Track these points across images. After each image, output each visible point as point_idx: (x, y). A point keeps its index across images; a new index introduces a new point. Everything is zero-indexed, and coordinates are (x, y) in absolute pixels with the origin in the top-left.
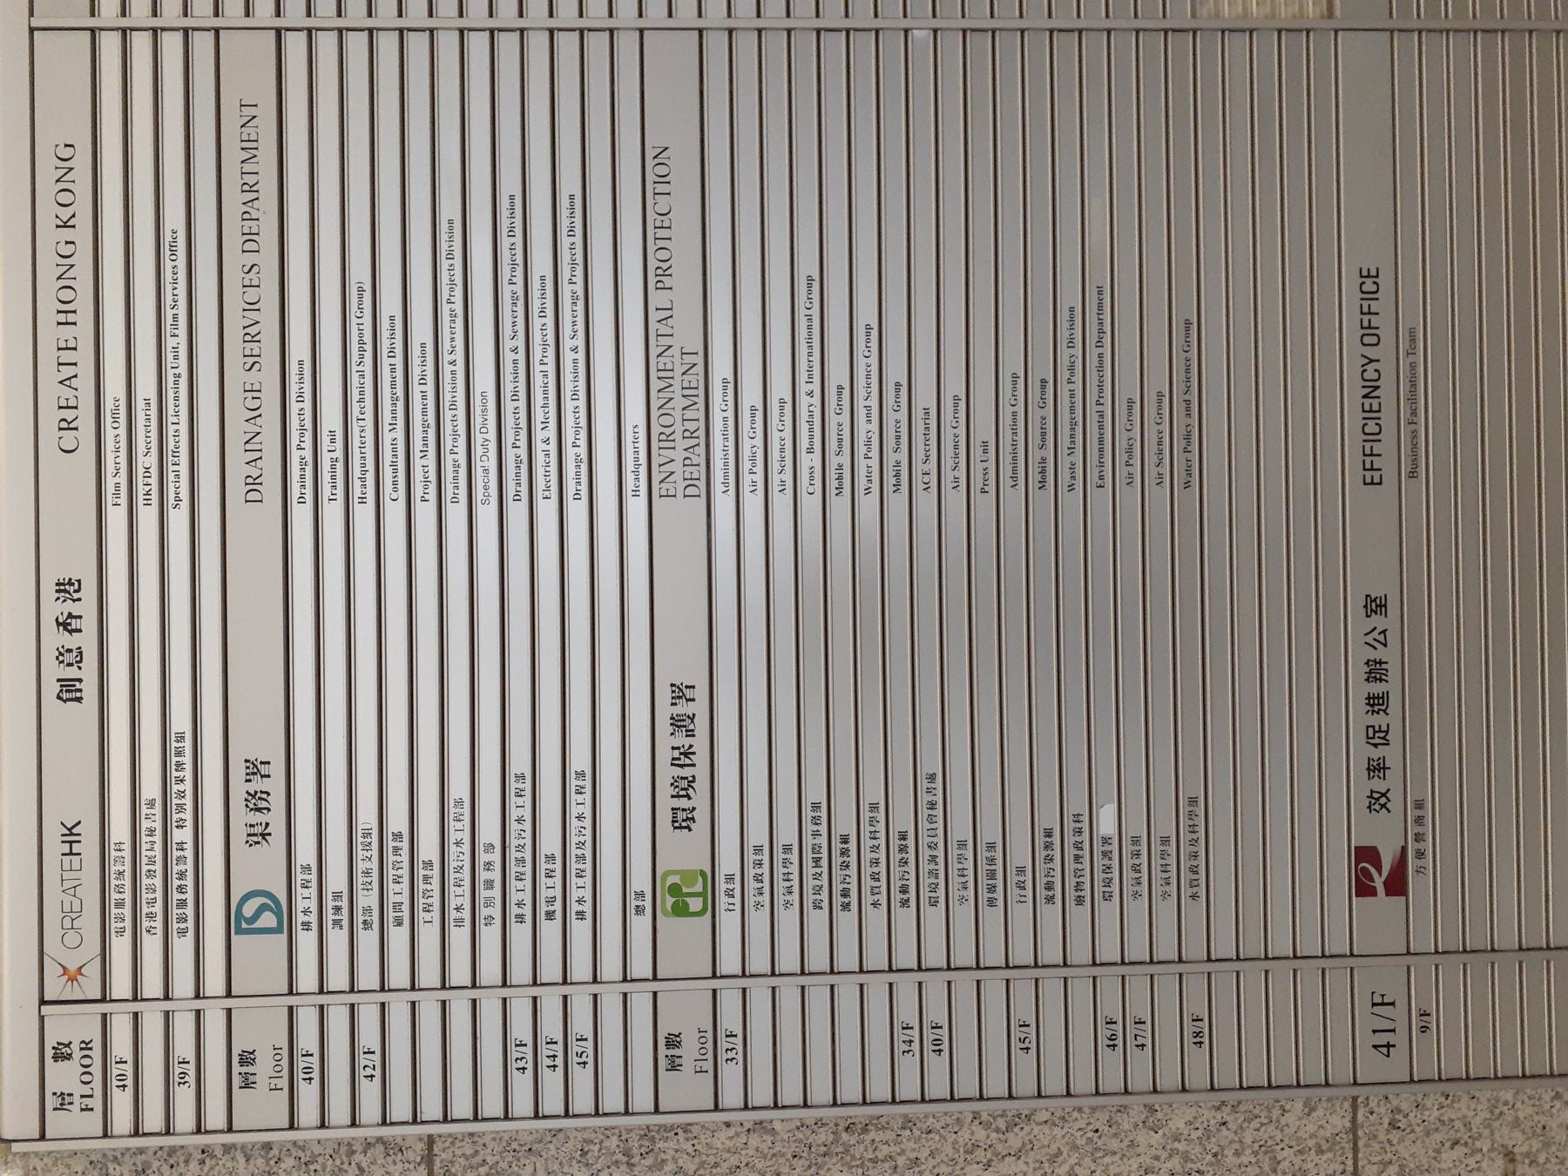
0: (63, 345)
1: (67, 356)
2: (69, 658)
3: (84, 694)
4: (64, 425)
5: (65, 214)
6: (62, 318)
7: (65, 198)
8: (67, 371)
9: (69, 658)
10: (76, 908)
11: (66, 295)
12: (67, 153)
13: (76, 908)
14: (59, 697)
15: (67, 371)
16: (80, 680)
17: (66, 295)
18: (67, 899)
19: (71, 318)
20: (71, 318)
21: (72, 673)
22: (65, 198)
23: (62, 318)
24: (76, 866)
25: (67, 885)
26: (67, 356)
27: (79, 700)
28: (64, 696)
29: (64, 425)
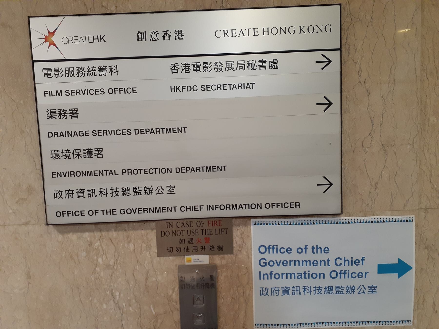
0: (256, 30)
1: (251, 32)
2: (154, 36)
3: (140, 41)
4: (226, 32)
5: (305, 30)
6: (266, 30)
7: (311, 29)
8: (246, 33)
9: (154, 36)
10: (76, 41)
11: (274, 31)
12: (328, 29)
13: (76, 41)
14: (139, 32)
15: (246, 33)
16: (146, 40)
17: (274, 31)
18: (79, 38)
19: (266, 33)
20: (266, 33)
21: (148, 37)
22: (311, 29)
23: (266, 30)
24: (90, 41)
25: (84, 38)
26: (251, 32)
27: (138, 40)
28: (140, 35)
29: (226, 32)
